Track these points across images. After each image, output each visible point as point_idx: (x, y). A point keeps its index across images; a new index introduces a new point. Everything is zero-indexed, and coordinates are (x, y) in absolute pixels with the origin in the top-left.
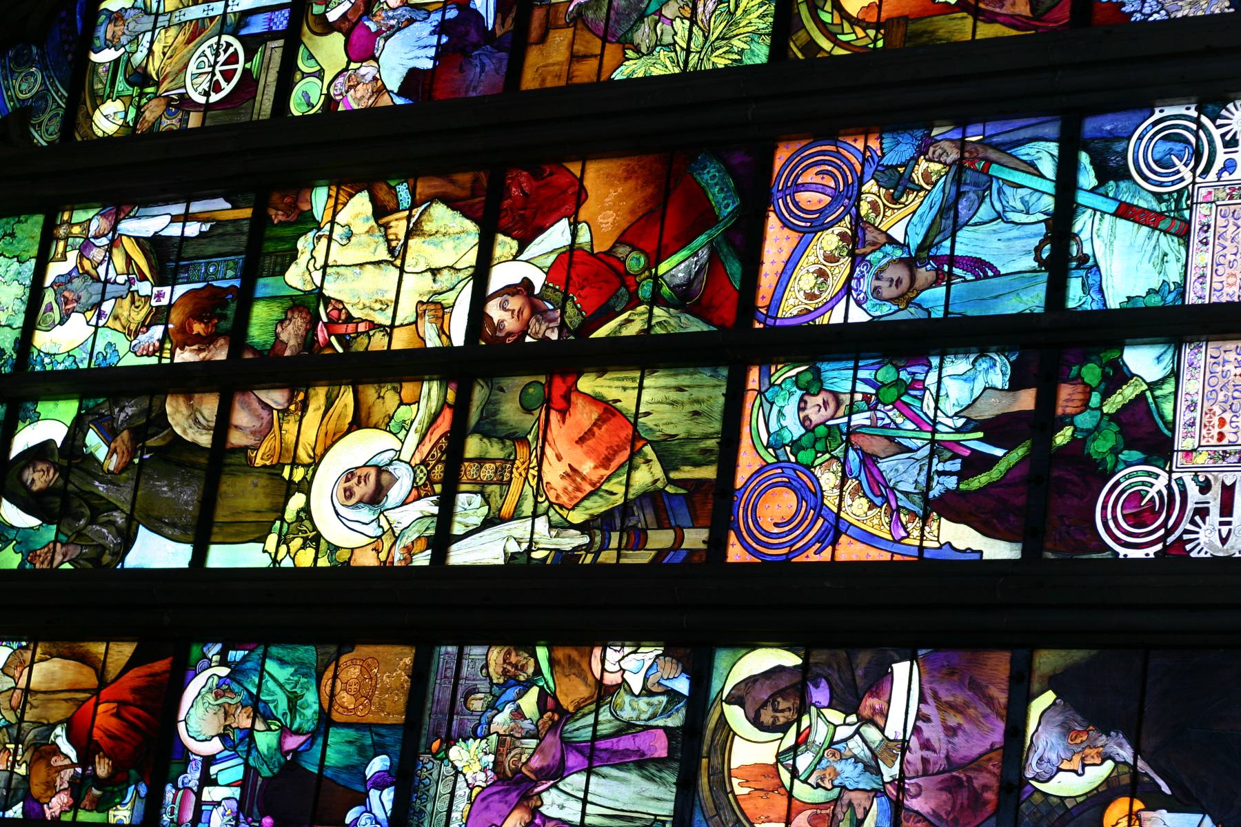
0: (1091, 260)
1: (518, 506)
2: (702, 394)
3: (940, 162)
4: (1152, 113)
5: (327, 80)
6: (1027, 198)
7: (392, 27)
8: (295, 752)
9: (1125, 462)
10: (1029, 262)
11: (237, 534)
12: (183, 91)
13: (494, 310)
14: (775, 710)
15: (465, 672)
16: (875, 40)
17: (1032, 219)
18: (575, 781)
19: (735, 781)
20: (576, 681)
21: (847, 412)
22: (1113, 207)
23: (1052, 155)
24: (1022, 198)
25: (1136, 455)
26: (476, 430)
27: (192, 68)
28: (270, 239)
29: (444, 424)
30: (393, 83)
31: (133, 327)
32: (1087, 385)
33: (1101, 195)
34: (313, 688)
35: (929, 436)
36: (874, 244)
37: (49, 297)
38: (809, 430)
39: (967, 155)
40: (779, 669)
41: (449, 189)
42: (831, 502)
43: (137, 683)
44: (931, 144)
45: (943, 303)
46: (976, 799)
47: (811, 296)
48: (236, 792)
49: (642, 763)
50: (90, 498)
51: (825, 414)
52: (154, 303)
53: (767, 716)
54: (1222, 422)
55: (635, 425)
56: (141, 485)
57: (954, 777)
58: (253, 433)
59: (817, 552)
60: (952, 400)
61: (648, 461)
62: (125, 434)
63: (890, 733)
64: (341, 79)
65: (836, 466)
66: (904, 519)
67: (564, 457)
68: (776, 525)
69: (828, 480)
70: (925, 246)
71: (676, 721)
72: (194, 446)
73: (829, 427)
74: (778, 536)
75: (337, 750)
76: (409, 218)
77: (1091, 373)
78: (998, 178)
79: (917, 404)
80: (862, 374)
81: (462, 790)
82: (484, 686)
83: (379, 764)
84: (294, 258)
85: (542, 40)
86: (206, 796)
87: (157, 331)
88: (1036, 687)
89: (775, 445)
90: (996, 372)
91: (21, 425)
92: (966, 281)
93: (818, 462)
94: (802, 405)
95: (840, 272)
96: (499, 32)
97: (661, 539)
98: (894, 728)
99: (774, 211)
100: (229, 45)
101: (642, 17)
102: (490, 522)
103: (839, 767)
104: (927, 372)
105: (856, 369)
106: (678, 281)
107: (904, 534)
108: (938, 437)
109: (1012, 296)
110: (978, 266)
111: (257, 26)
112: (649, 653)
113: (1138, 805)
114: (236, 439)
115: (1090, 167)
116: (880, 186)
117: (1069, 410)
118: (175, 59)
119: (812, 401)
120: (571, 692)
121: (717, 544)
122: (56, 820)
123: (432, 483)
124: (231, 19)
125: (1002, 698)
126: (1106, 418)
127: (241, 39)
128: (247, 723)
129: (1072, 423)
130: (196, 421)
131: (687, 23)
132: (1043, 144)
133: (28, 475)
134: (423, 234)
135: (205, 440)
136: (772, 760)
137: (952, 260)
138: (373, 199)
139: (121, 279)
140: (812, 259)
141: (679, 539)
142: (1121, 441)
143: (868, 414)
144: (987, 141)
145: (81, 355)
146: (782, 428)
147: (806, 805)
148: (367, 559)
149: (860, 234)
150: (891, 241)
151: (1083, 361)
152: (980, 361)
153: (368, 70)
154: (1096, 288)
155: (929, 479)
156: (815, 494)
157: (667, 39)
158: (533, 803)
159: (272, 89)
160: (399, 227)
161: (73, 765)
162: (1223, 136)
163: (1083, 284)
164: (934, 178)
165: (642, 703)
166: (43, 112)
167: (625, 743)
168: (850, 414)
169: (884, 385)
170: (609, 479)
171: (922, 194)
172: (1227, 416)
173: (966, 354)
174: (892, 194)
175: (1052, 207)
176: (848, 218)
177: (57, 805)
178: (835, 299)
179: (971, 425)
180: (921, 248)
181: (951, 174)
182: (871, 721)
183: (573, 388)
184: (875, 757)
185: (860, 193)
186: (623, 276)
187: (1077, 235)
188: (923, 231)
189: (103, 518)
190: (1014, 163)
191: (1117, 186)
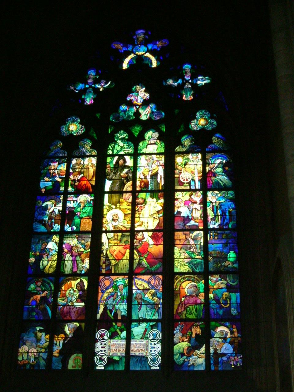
1: (110, 243)
2: (125, 269)
5: (182, 198)
7: (189, 207)
8: (77, 214)
10: (140, 316)
11: (110, 198)
12: (183, 172)
13: (141, 233)
15: (87, 239)
16: (177, 289)
17: (146, 316)
18: (71, 258)
19: (69, 282)
20: (85, 256)
22: (147, 328)
25: (110, 334)
26: (122, 234)
27: (186, 173)
28: (156, 194)
29: (124, 229)
30: (179, 210)
34: (86, 215)
37: (150, 156)
38: (118, 286)
40: (84, 286)
41: (161, 222)
42: (108, 291)
43: (89, 186)
46: (66, 316)
47: (138, 284)
48: (72, 206)
49: (73, 268)
50: (117, 172)
51: (120, 288)
53: (78, 285)
54: (114, 346)
55: (121, 259)
56: (119, 180)
57: (69, 313)
58: (125, 197)
59: (100, 290)
60: (121, 307)
61: (115, 262)
62: (127, 175)
64: (181, 200)
66: (104, 302)
67: (117, 248)
69: (110, 290)
70: (144, 301)
71: (78, 272)
72: (124, 188)
75: (77, 221)
76: (157, 217)
77: (123, 327)
79: (120, 302)
80: (125, 293)
81: (70, 241)
82: (85, 242)
83: (75, 228)
84: (152, 198)
85: (184, 234)
86: (71, 201)
87: (142, 177)
88: (80, 323)
89: (117, 281)
90: (124, 313)
91: (130, 157)
96: (186, 226)
97: (104, 266)
100: (189, 179)
101: (186, 250)
102: (108, 239)
103: (71, 297)
106: (142, 263)
108: (115, 305)
110: (140, 308)
111: (192, 183)
112: (88, 267)
113: (64, 338)
114: (124, 194)
118: (189, 170)
119: (122, 286)
120: (83, 256)
121: (102, 275)
122: (69, 178)
123: (115, 229)
124: (194, 178)
125: (79, 319)
127: (190, 182)
128: (82, 206)
130: (128, 187)
131: (184, 258)
132: (157, 317)
133: (122, 160)
134: (154, 219)
135: (125, 190)
137: (141, 305)
138: (161, 210)
139: (152, 169)
140: (144, 283)
141: (104, 269)
143: (120, 295)
147: (66, 292)
148: (104, 220)
150: (145, 295)
151: (125, 326)
153: (183, 204)
155: (109, 305)
157: (181, 255)
158: (68, 253)
159: (181, 188)
160: (155, 215)
161: (77, 178)
162: (156, 343)
165: (81, 267)
166: (182, 147)
167: (76, 265)
170: (113, 256)
172: (115, 347)
173: (128, 308)
175: (148, 319)
177: (72, 177)
179: (116, 310)
180: (144, 300)
183: (127, 248)
185: (153, 289)
186: (144, 254)
189: (114, 175)
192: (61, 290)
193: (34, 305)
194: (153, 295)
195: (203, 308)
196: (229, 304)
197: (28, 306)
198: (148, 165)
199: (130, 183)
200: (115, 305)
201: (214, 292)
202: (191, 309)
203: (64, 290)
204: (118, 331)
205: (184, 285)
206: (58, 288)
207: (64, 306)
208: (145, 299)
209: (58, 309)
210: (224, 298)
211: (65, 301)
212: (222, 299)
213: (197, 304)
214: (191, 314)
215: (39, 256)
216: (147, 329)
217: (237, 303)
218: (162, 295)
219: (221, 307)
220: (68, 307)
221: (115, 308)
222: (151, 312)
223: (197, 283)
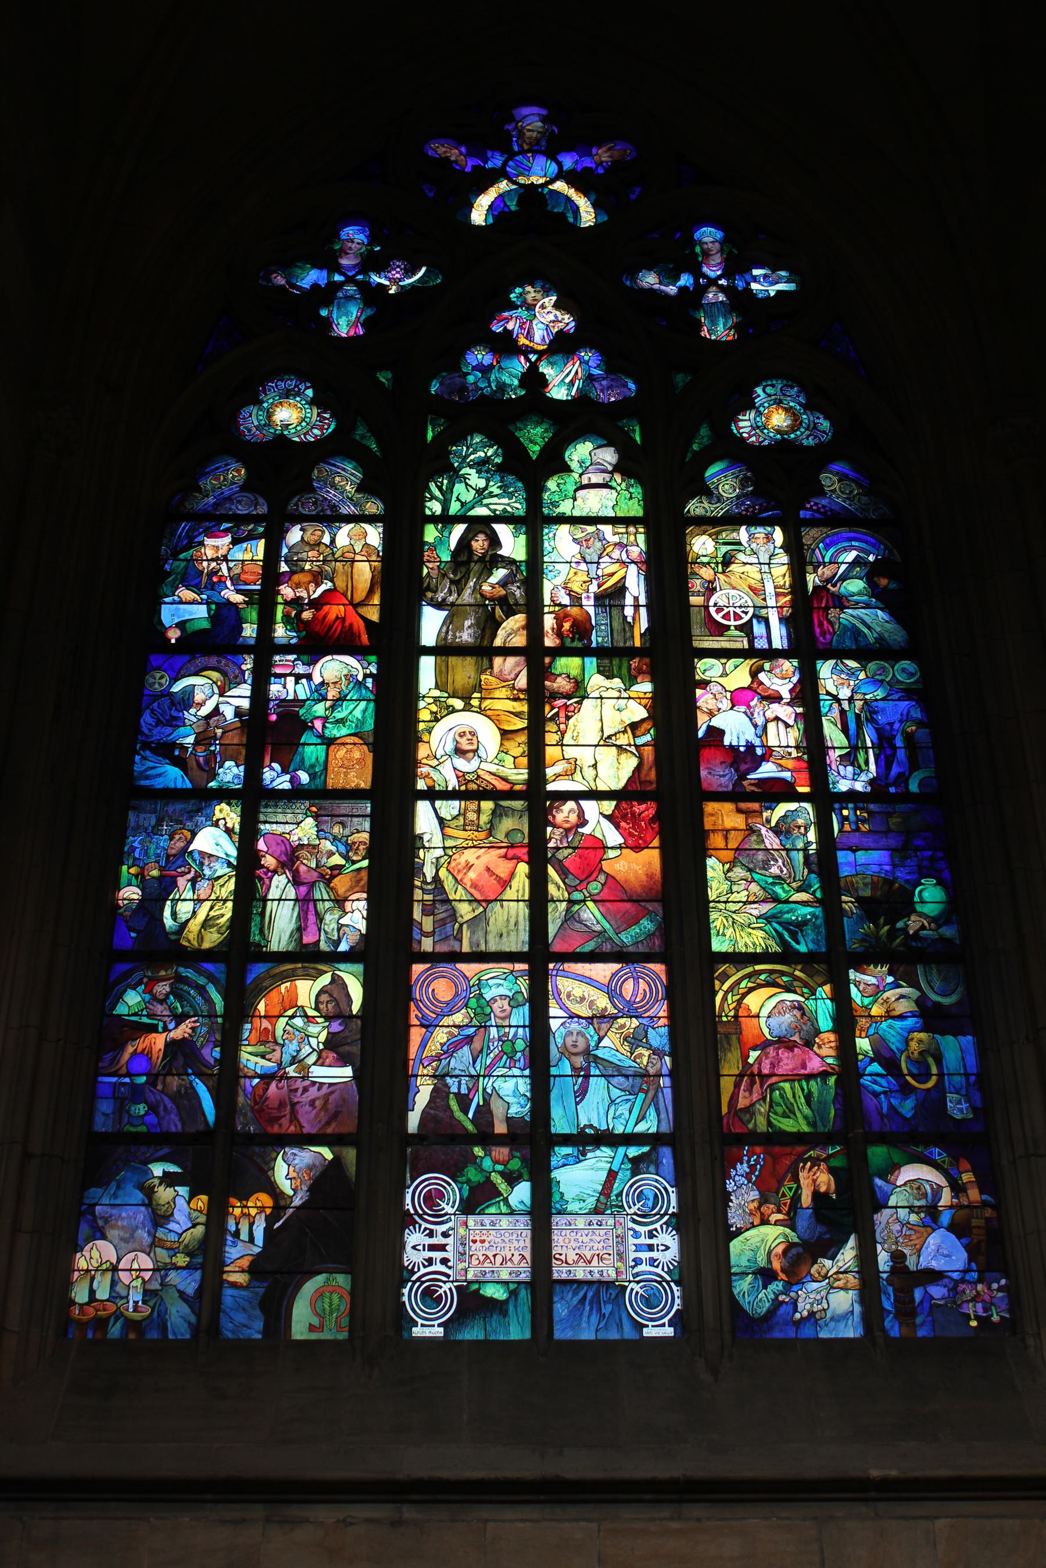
14: (327, 1002)
16: (726, 1016)
19: (288, 984)
31: (569, 585)
36: (599, 1029)
37: (591, 529)
40: (350, 1001)
42: (446, 1021)
47: (569, 996)
51: (497, 1011)
52: (583, 596)
53: (324, 998)
63: (313, 1069)
65: (466, 1021)
68: (433, 990)
69: (458, 1018)
74: (427, 992)
79: (502, 1064)
87: (566, 600)
91: (511, 527)
95: (584, 1011)
98: (317, 1071)
103: (295, 1042)
105: (524, 1027)
108: (481, 1079)
136: (299, 1004)
137: (587, 1076)
139: (600, 573)
140: (592, 993)
145: (554, 557)
147: (274, 1026)
150: (600, 1039)
155: (456, 1076)
168: (497, 1026)
169: (513, 1044)
173: (532, 1090)
178: (566, 1009)
180: (596, 1056)
182: (319, 1057)
184: (300, 1061)
185: (631, 1017)
192: (253, 1016)
193: (139, 1075)
194: (635, 1040)
195: (836, 1093)
196: (934, 1079)
197: (114, 1080)
198: (584, 558)
199: (518, 620)
200: (479, 1076)
201: (872, 1031)
202: (790, 1095)
203: (265, 1017)
205: (753, 1001)
206: (240, 1009)
207: (267, 1078)
209: (241, 1092)
210: (916, 1053)
211: (269, 1060)
212: (908, 1057)
213: (809, 1077)
214: (789, 1113)
215: (160, 883)
217: (966, 1075)
218: (670, 1040)
219: (905, 1090)
220: (284, 1082)
221: (481, 1090)
222: (630, 1103)
223: (802, 996)
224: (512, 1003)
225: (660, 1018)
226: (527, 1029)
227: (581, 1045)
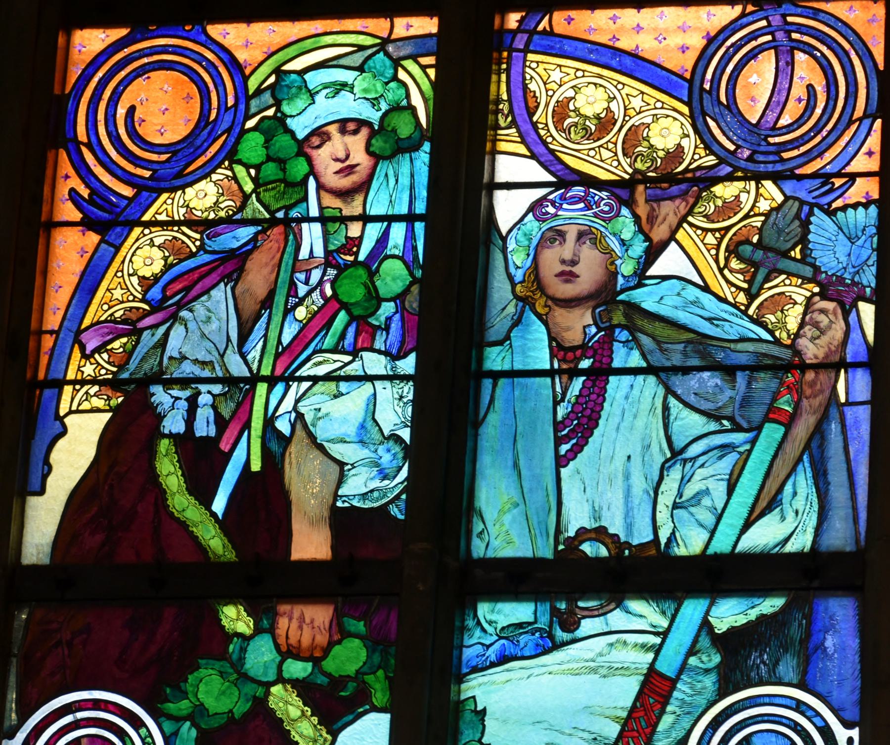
0: (566, 636)
3: (802, 326)
4: (848, 725)
6: (706, 502)
9: (176, 733)
10: (577, 518)
17: (663, 515)
21: (328, 213)
22: (667, 666)
23: (787, 540)
24: (707, 492)
32: (326, 651)
33: (695, 641)
35: (266, 371)
38: (302, 148)
39: (810, 375)
42: (164, 206)
44: (842, 304)
45: (518, 366)
47: (561, 112)
68: (132, 110)
69: (203, 196)
73: (304, 182)
77: (349, 657)
78: (753, 442)
79: (329, 342)
90: (372, 480)
92: (556, 403)
93: (240, 170)
94: (351, 126)
99: (743, 15)
104: (386, 353)
107: (89, 348)
108: (262, 388)
109: (517, 498)
115: (753, 615)
116: (767, 215)
117: (283, 623)
119: (356, 145)
126: (260, 692)
129: (258, 630)
137: (601, 373)
140: (637, 103)
142: (215, 723)
143: (319, 252)
144: (834, 412)
146: (312, 95)
149: (675, 189)
150: (653, 252)
152: (397, 449)
154: (511, 650)
155: (185, 382)
156: (180, 175)
163: (520, 625)
164: (771, 318)
168: (323, 220)
171: (742, 298)
174: (748, 242)
175: (681, 551)
176: (711, 160)
179: (276, 446)
180: (633, 308)
181: (775, 351)
185: (758, 178)
187: (619, 604)
188: (664, 310)
190: (781, 470)
191: (707, 671)
200: (254, 379)
204: (287, 704)
208: (649, 305)
216: (672, 683)
222: (731, 459)
224: (378, 144)
225: (852, 177)
226: (419, 227)
227: (589, 271)
